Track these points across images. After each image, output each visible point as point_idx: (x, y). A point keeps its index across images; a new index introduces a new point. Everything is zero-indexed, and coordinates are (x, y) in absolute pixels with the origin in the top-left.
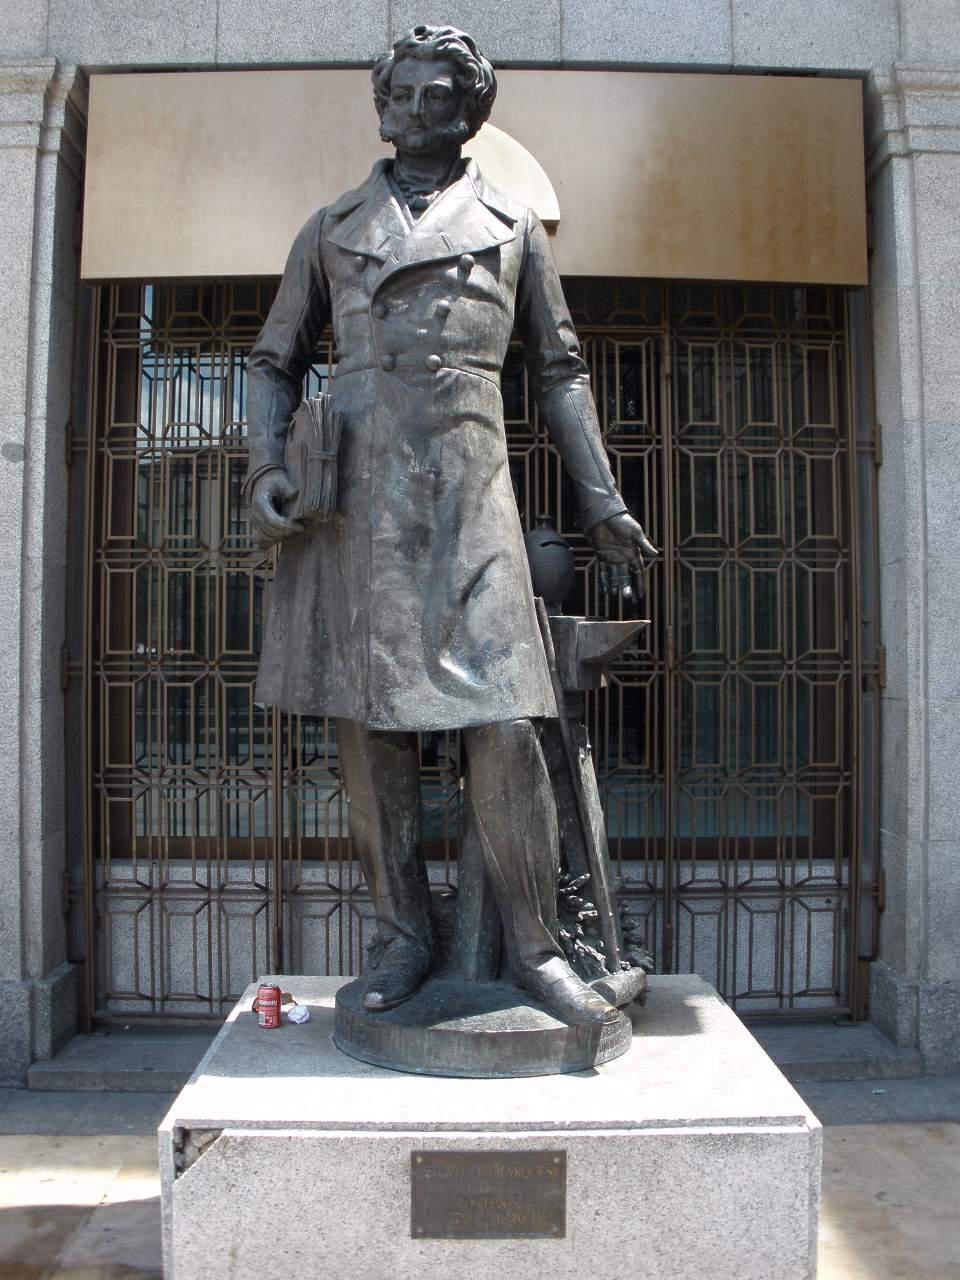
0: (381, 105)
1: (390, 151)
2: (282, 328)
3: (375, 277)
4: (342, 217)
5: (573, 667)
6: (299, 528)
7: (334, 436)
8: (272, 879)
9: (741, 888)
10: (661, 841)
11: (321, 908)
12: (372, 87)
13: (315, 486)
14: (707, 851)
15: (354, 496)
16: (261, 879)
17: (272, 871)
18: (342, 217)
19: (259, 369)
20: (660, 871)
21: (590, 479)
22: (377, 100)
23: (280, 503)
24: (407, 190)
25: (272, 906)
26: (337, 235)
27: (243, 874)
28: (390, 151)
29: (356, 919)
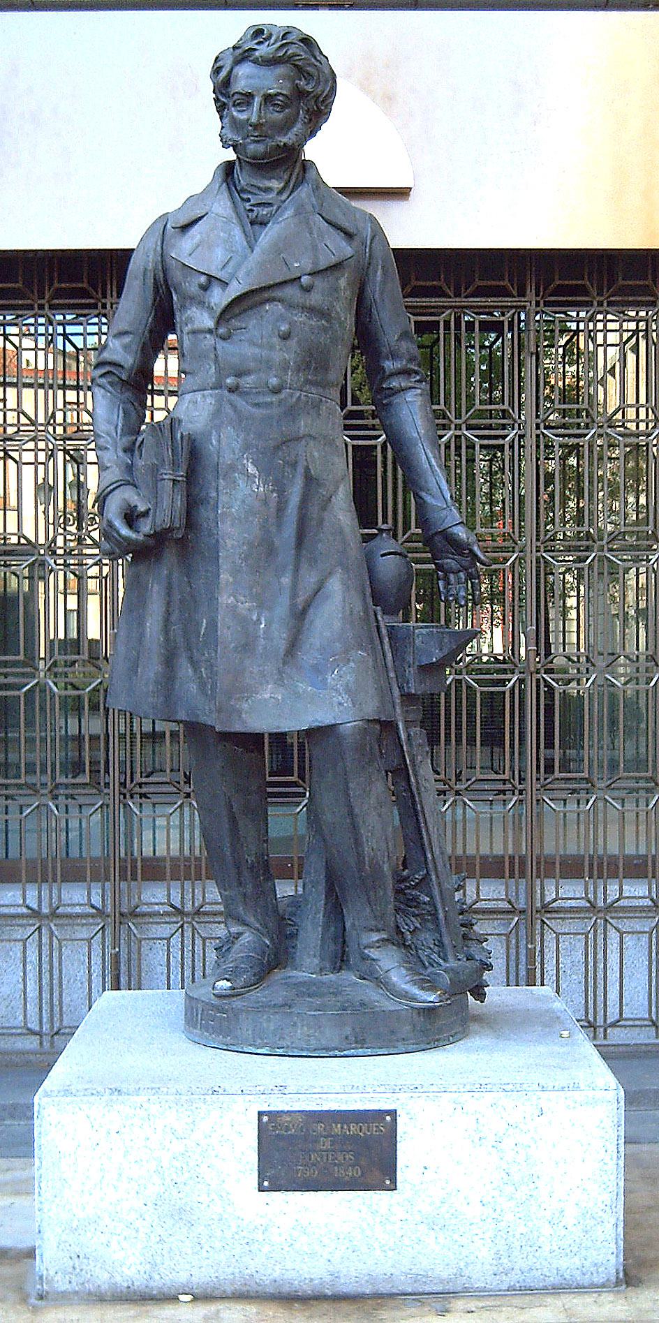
0: (221, 108)
1: (230, 155)
2: (127, 339)
3: (219, 298)
4: (185, 228)
5: (411, 672)
6: (152, 542)
7: (183, 457)
8: (109, 902)
9: (609, 908)
10: (522, 860)
11: (164, 930)
12: (210, 86)
13: (166, 503)
14: (572, 868)
15: (204, 513)
16: (97, 900)
17: (109, 894)
18: (185, 228)
19: (103, 381)
20: (522, 887)
21: (428, 491)
22: (216, 100)
23: (131, 517)
24: (249, 200)
25: (108, 931)
26: (184, 249)
27: (75, 896)
28: (230, 155)
29: (198, 942)
